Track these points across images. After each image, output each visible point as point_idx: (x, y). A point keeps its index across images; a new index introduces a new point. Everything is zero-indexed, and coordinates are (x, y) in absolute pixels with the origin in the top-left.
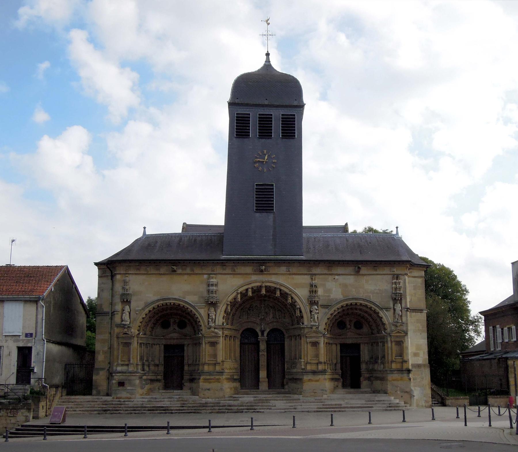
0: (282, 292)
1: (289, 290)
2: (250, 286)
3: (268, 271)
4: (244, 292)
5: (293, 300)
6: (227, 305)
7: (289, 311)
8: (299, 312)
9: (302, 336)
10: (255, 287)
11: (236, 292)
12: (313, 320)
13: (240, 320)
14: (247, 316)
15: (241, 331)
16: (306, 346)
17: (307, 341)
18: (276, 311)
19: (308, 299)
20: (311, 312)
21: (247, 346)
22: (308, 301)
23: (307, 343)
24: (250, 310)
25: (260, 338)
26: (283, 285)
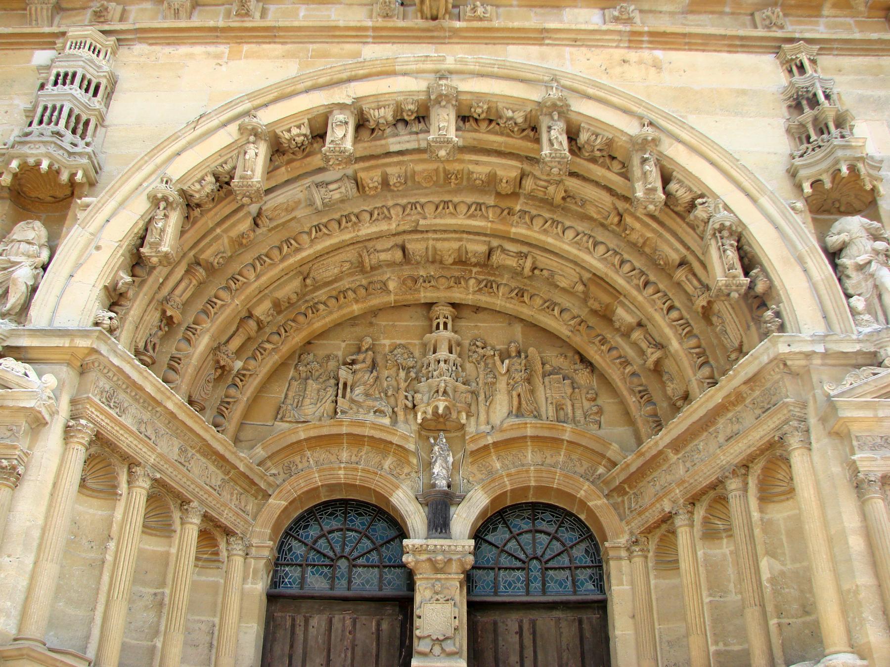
0: (583, 137)
1: (641, 118)
2: (343, 95)
3: (481, 19)
4: (295, 131)
5: (673, 187)
6: (155, 201)
7: (626, 363)
8: (732, 255)
9: (794, 441)
10: (378, 101)
11: (233, 128)
12: (869, 309)
13: (285, 425)
14: (328, 406)
15: (277, 503)
16: (850, 519)
17: (854, 469)
18: (538, 381)
19: (793, 173)
20: (834, 256)
21: (318, 622)
22: (799, 187)
23: (859, 486)
24: (353, 362)
25: (417, 551)
26: (591, 91)
